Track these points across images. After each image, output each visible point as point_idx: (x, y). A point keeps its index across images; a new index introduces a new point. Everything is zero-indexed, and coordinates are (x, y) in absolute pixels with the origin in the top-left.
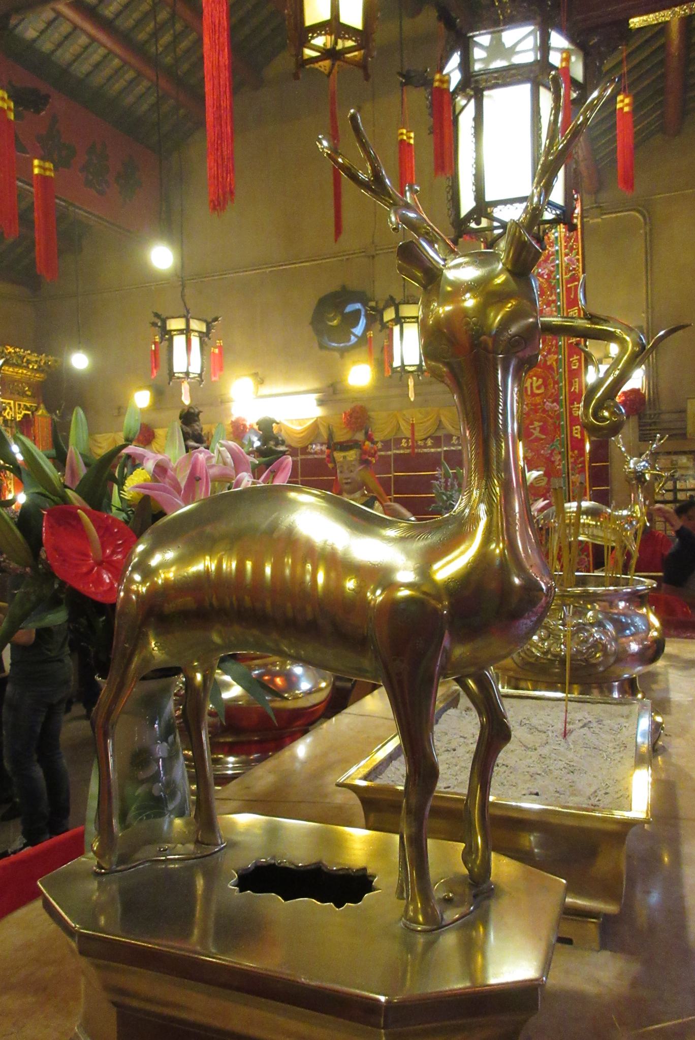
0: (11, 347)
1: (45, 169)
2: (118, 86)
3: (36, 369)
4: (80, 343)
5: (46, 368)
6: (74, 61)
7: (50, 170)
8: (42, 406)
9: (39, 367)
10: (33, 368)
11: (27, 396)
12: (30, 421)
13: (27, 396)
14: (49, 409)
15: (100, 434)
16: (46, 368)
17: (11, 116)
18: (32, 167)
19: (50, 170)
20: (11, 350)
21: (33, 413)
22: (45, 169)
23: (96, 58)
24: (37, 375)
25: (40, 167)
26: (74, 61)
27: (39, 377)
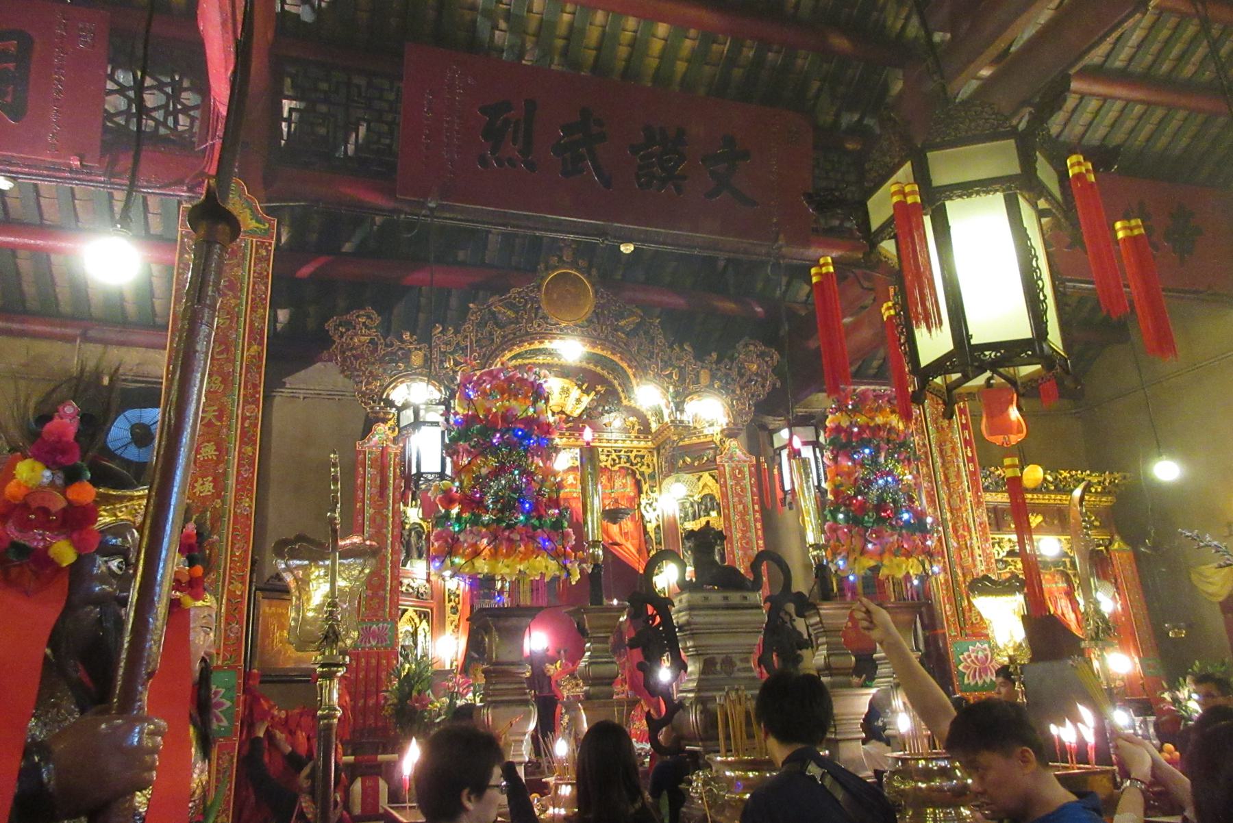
0: (1065, 471)
1: (1131, 229)
2: (1142, 137)
3: (1101, 493)
4: (1159, 446)
5: (1114, 489)
6: (1086, 131)
7: (1138, 227)
8: (1116, 537)
9: (1104, 488)
10: (1096, 492)
11: (1096, 527)
12: (1106, 558)
13: (1096, 527)
14: (1126, 539)
15: (1204, 564)
16: (1114, 489)
17: (1092, 178)
18: (1115, 232)
19: (1138, 227)
20: (1066, 474)
21: (1107, 548)
22: (1131, 229)
23: (1113, 115)
24: (1104, 499)
25: (1124, 228)
26: (1086, 131)
27: (1106, 501)
